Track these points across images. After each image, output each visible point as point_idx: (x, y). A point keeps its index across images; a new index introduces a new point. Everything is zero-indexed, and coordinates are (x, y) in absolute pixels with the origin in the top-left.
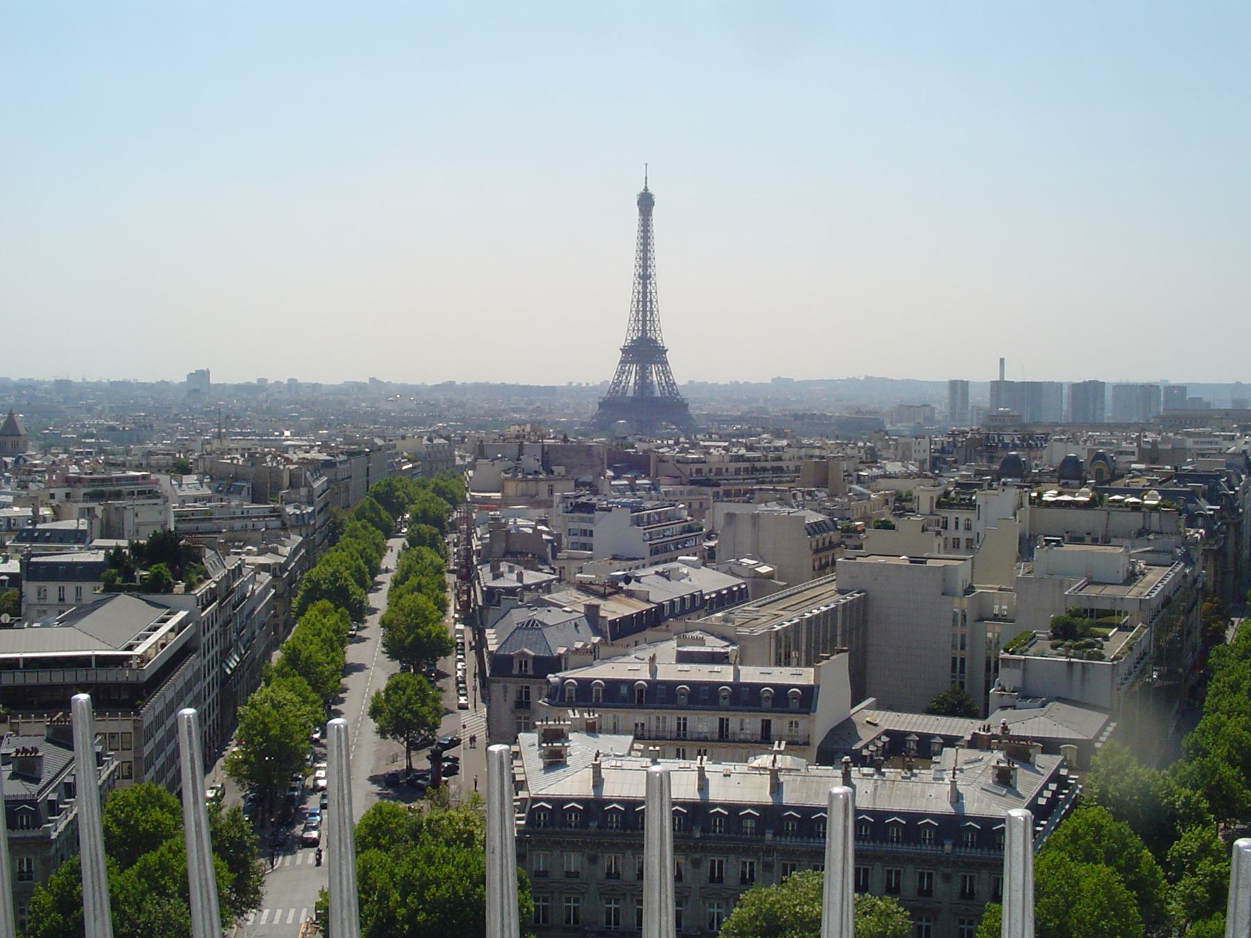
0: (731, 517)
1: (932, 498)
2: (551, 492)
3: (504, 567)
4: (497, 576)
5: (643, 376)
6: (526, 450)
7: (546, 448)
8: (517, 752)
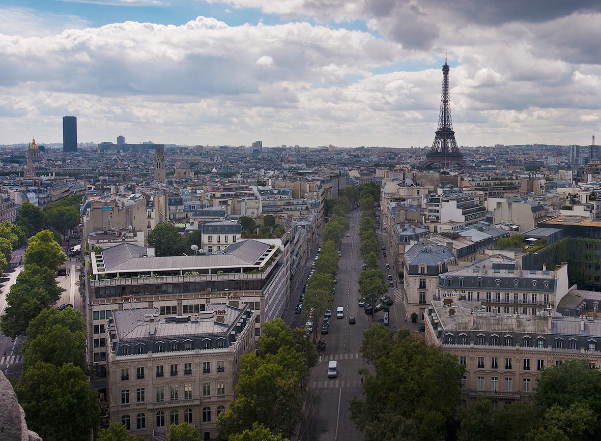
0: (499, 204)
1: (587, 196)
2: (418, 193)
3: (406, 226)
4: (404, 230)
5: (445, 144)
6: (406, 176)
7: (414, 174)
8: (432, 309)
